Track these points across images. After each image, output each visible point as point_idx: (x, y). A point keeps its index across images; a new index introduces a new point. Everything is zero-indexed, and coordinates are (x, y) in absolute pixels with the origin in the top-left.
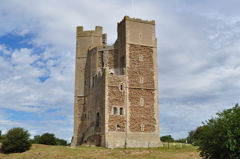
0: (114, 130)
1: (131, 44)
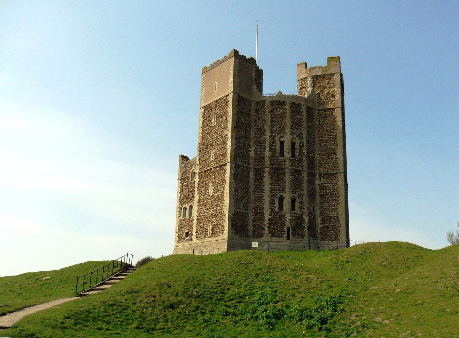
1: (205, 106)
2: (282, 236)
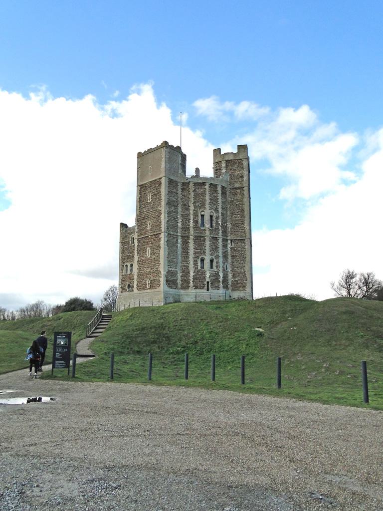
1: (141, 185)
2: (203, 288)
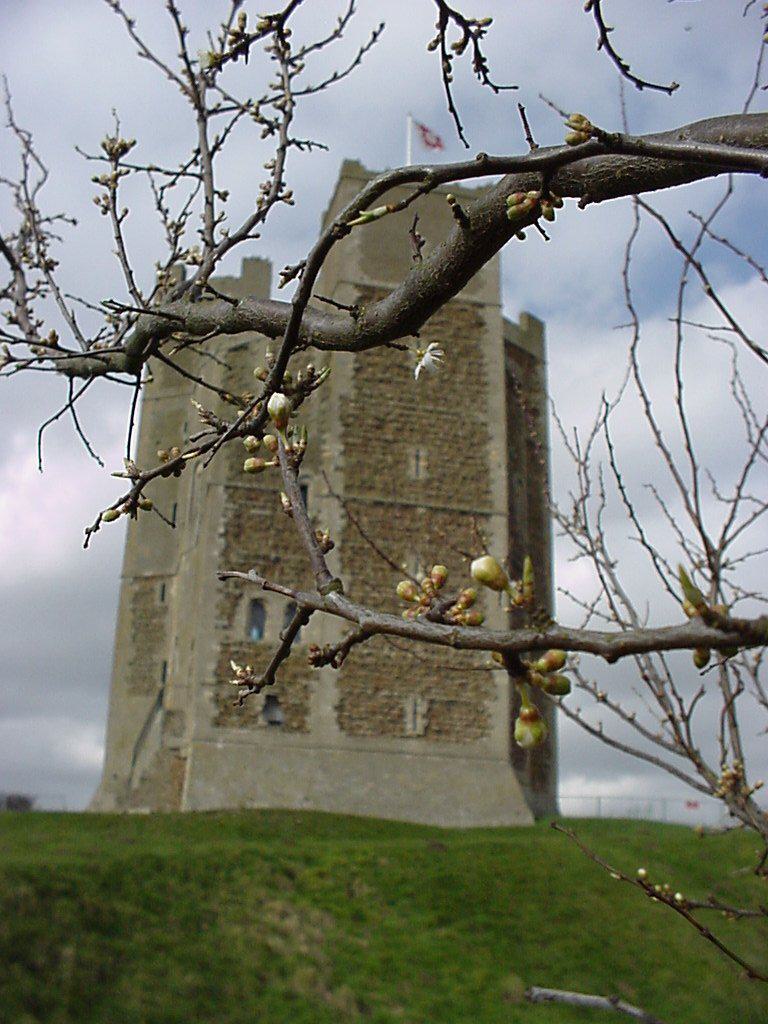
0: (248, 721)
